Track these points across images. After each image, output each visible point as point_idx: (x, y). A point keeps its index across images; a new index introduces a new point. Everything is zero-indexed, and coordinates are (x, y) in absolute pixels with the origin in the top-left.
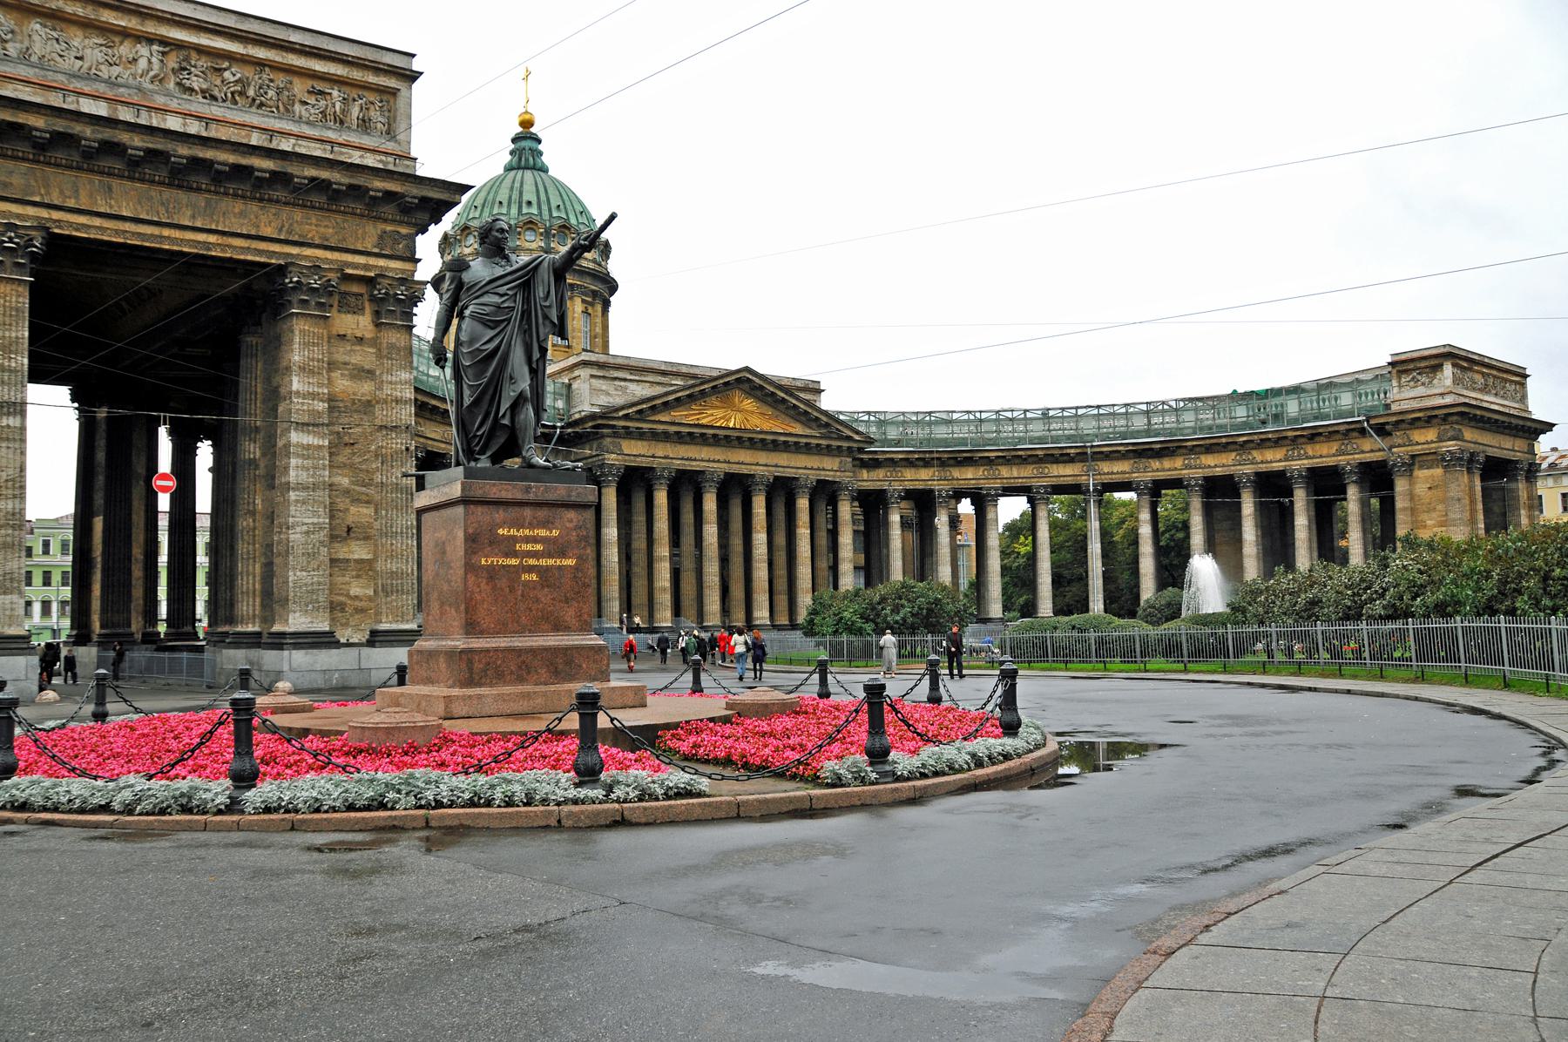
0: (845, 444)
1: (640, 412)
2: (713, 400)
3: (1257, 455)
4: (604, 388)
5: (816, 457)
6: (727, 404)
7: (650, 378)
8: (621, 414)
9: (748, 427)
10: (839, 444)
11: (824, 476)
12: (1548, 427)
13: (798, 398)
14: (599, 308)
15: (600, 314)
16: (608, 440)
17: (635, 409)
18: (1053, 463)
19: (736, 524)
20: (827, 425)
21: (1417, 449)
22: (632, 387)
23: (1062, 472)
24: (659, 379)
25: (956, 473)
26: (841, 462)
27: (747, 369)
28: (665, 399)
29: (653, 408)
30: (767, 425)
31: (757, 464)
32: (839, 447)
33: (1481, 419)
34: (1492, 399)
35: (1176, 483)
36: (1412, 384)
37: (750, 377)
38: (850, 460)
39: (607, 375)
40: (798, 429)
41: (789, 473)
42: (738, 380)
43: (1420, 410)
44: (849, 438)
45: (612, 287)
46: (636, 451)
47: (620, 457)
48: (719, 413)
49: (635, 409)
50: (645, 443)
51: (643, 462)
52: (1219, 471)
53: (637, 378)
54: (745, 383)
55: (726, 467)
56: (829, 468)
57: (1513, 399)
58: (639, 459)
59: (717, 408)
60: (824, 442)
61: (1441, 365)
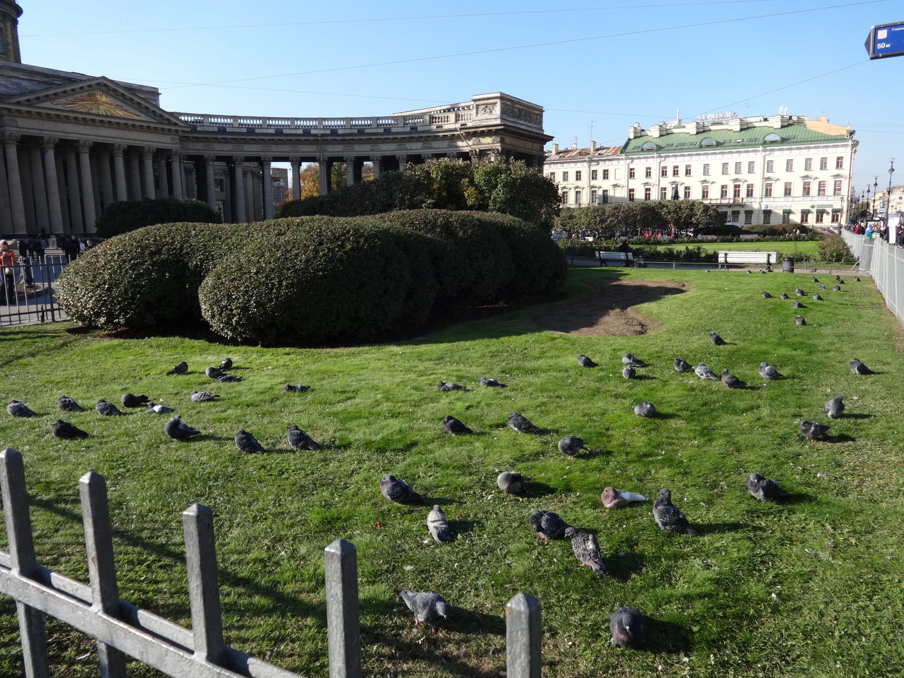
0: (173, 128)
1: (29, 100)
3: (408, 145)
4: (3, 82)
6: (92, 97)
7: (37, 79)
8: (14, 101)
9: (109, 114)
11: (160, 146)
12: (550, 138)
13: (140, 97)
14: (9, 25)
15: (9, 29)
16: (7, 117)
17: (24, 98)
18: (300, 144)
19: (136, 173)
21: (483, 147)
22: (25, 83)
23: (305, 150)
24: (44, 79)
25: (246, 147)
26: (172, 139)
27: (104, 78)
29: (38, 98)
30: (121, 113)
32: (170, 130)
33: (514, 133)
34: (523, 122)
35: (341, 159)
36: (483, 112)
38: (177, 137)
39: (4, 74)
40: (144, 117)
41: (138, 143)
42: (98, 84)
43: (484, 127)
44: (175, 124)
45: (19, 11)
47: (17, 129)
51: (36, 133)
52: (388, 153)
53: (27, 78)
54: (105, 85)
56: (164, 141)
57: (535, 123)
58: (32, 131)
60: (160, 126)
61: (496, 103)
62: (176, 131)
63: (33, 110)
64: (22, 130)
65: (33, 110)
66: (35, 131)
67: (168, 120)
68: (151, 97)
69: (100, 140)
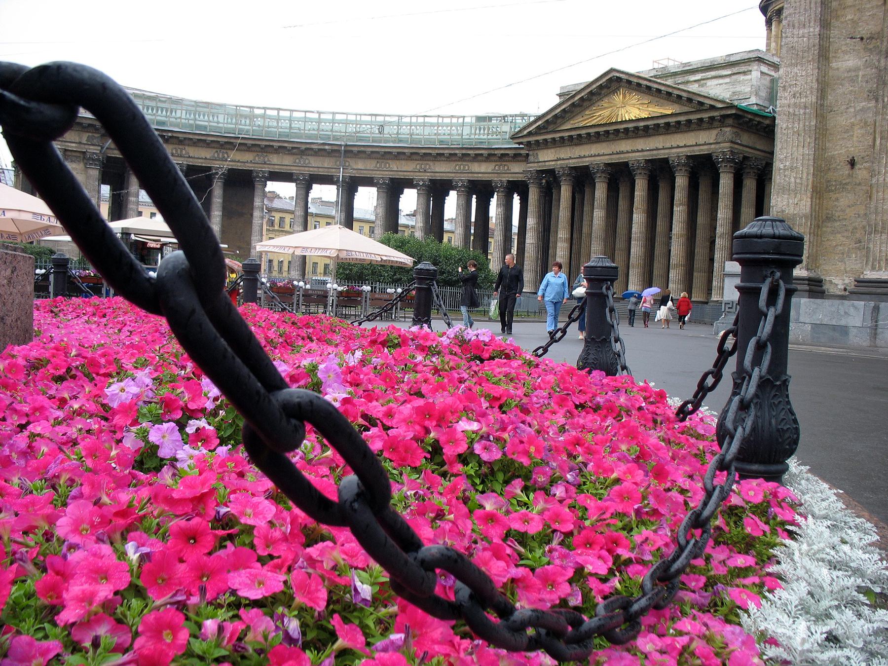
0: (705, 116)
2: (605, 103)
5: (692, 134)
8: (525, 132)
10: (699, 116)
11: (697, 151)
17: (534, 126)
20: (690, 100)
27: (612, 70)
28: (553, 114)
31: (633, 151)
37: (618, 75)
38: (728, 129)
42: (610, 80)
44: (712, 108)
46: (548, 158)
47: (536, 164)
48: (606, 113)
49: (534, 126)
50: (553, 150)
55: (606, 159)
58: (547, 164)
59: (605, 108)
60: (682, 119)
62: (712, 119)
63: (540, 138)
64: (540, 164)
65: (540, 138)
66: (551, 163)
67: (701, 104)
68: (743, 68)
69: (615, 159)
